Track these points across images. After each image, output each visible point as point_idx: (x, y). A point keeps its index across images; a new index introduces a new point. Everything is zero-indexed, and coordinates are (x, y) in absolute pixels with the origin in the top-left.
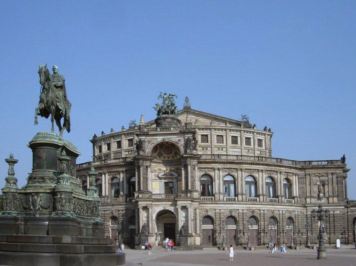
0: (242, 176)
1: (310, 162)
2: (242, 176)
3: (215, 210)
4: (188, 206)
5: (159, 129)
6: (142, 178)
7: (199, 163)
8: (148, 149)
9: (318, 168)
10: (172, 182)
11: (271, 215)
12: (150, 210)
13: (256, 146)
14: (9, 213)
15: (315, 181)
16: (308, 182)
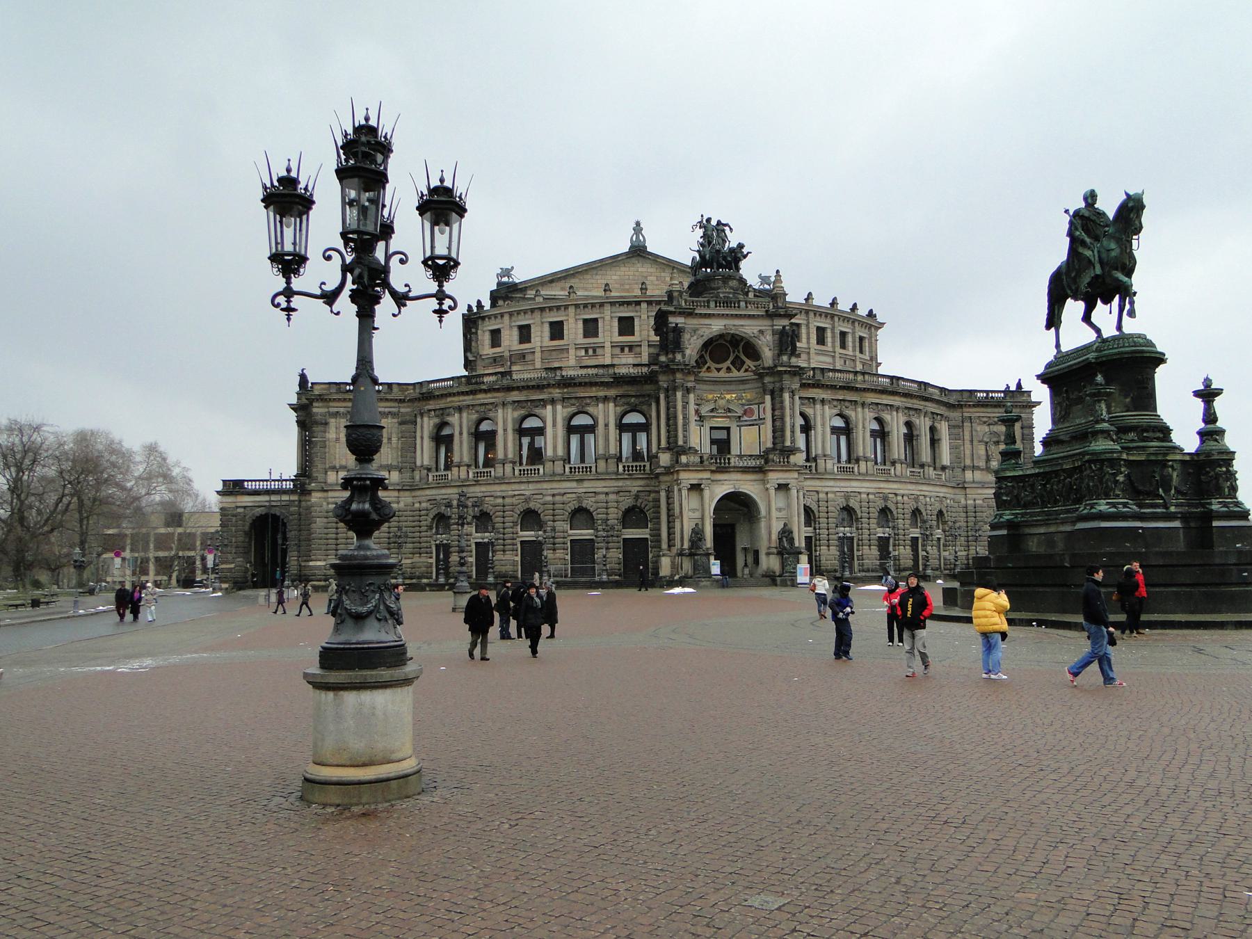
0: (864, 419)
1: (971, 392)
2: (864, 419)
3: (818, 492)
4: (793, 483)
5: (712, 304)
6: (680, 417)
7: (803, 386)
8: (692, 347)
9: (987, 406)
10: (728, 429)
11: (913, 505)
12: (707, 493)
13: (858, 353)
14: (1125, 505)
15: (981, 434)
16: (967, 437)
